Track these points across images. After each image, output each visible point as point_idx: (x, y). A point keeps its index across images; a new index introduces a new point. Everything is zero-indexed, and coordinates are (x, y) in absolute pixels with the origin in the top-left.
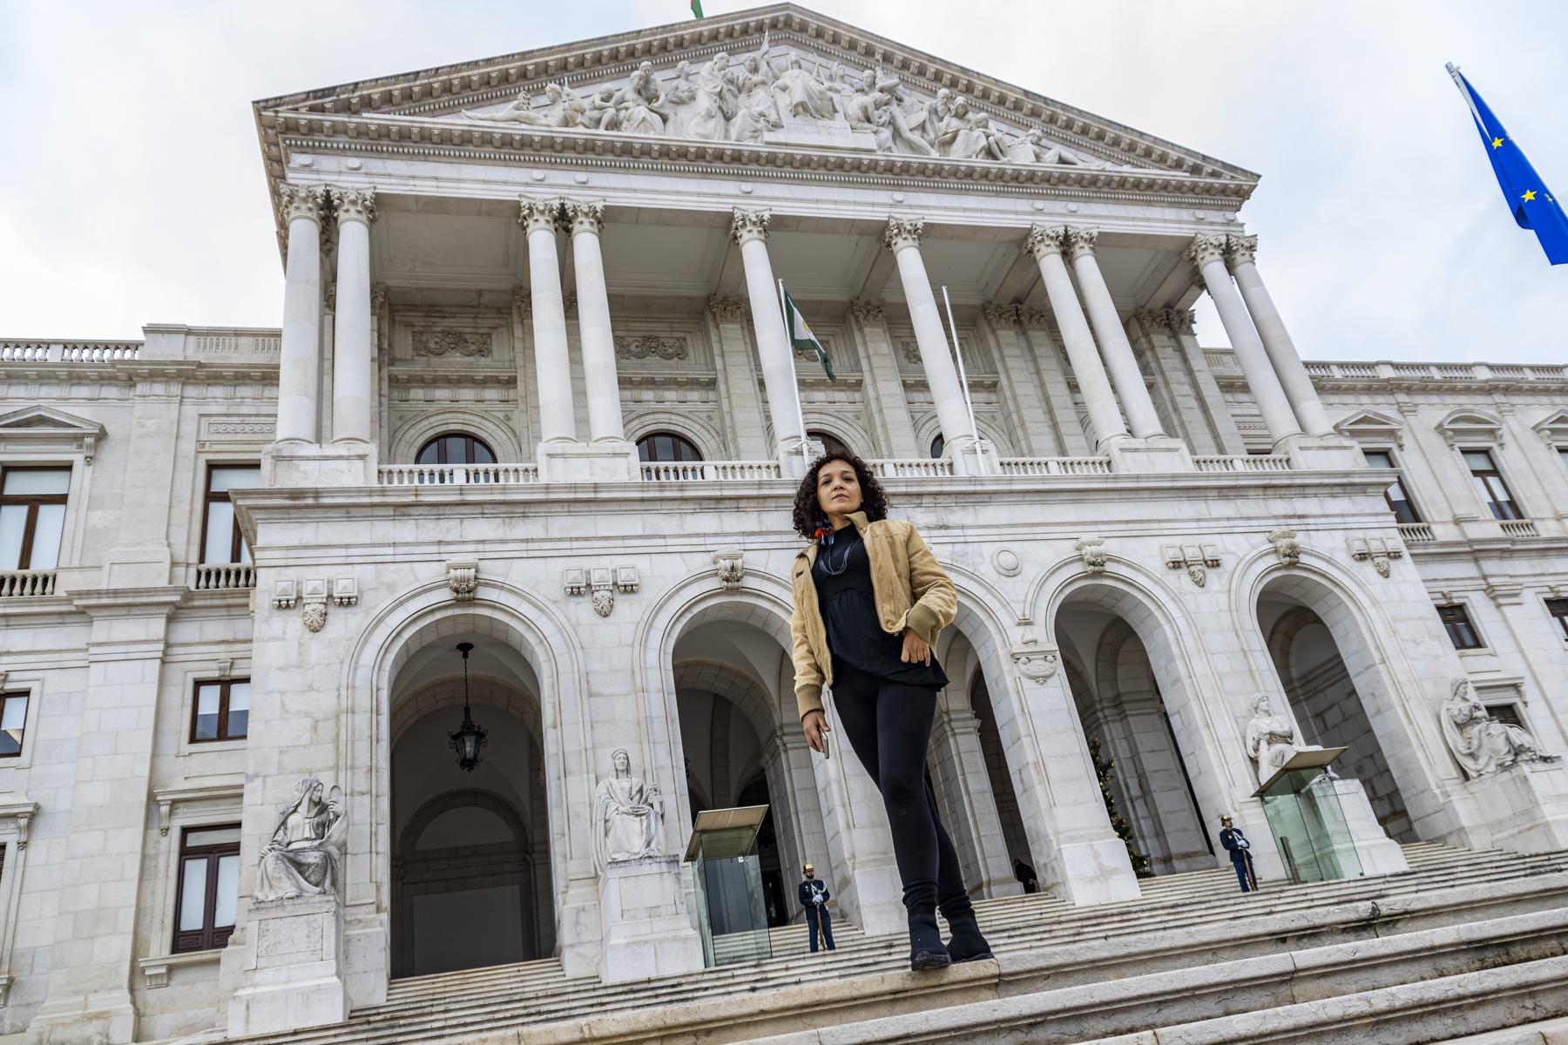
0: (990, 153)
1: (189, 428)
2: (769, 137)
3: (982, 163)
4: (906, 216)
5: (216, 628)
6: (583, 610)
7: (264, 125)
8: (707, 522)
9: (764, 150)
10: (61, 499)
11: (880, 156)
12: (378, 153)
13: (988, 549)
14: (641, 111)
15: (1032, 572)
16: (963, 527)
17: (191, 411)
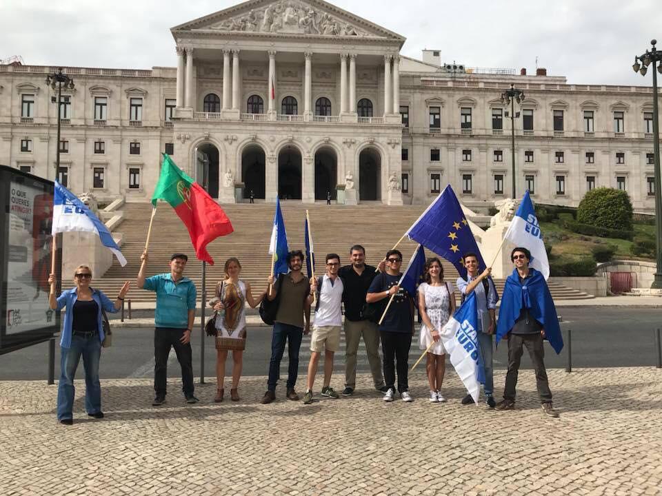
0: (334, 33)
1: (162, 91)
2: (278, 31)
3: (331, 36)
4: (309, 51)
5: (169, 134)
6: (227, 143)
7: (172, 33)
8: (251, 128)
9: (278, 35)
10: (141, 105)
11: (304, 36)
12: (194, 38)
13: (306, 137)
14: (249, 25)
15: (313, 142)
16: (301, 131)
17: (162, 87)
